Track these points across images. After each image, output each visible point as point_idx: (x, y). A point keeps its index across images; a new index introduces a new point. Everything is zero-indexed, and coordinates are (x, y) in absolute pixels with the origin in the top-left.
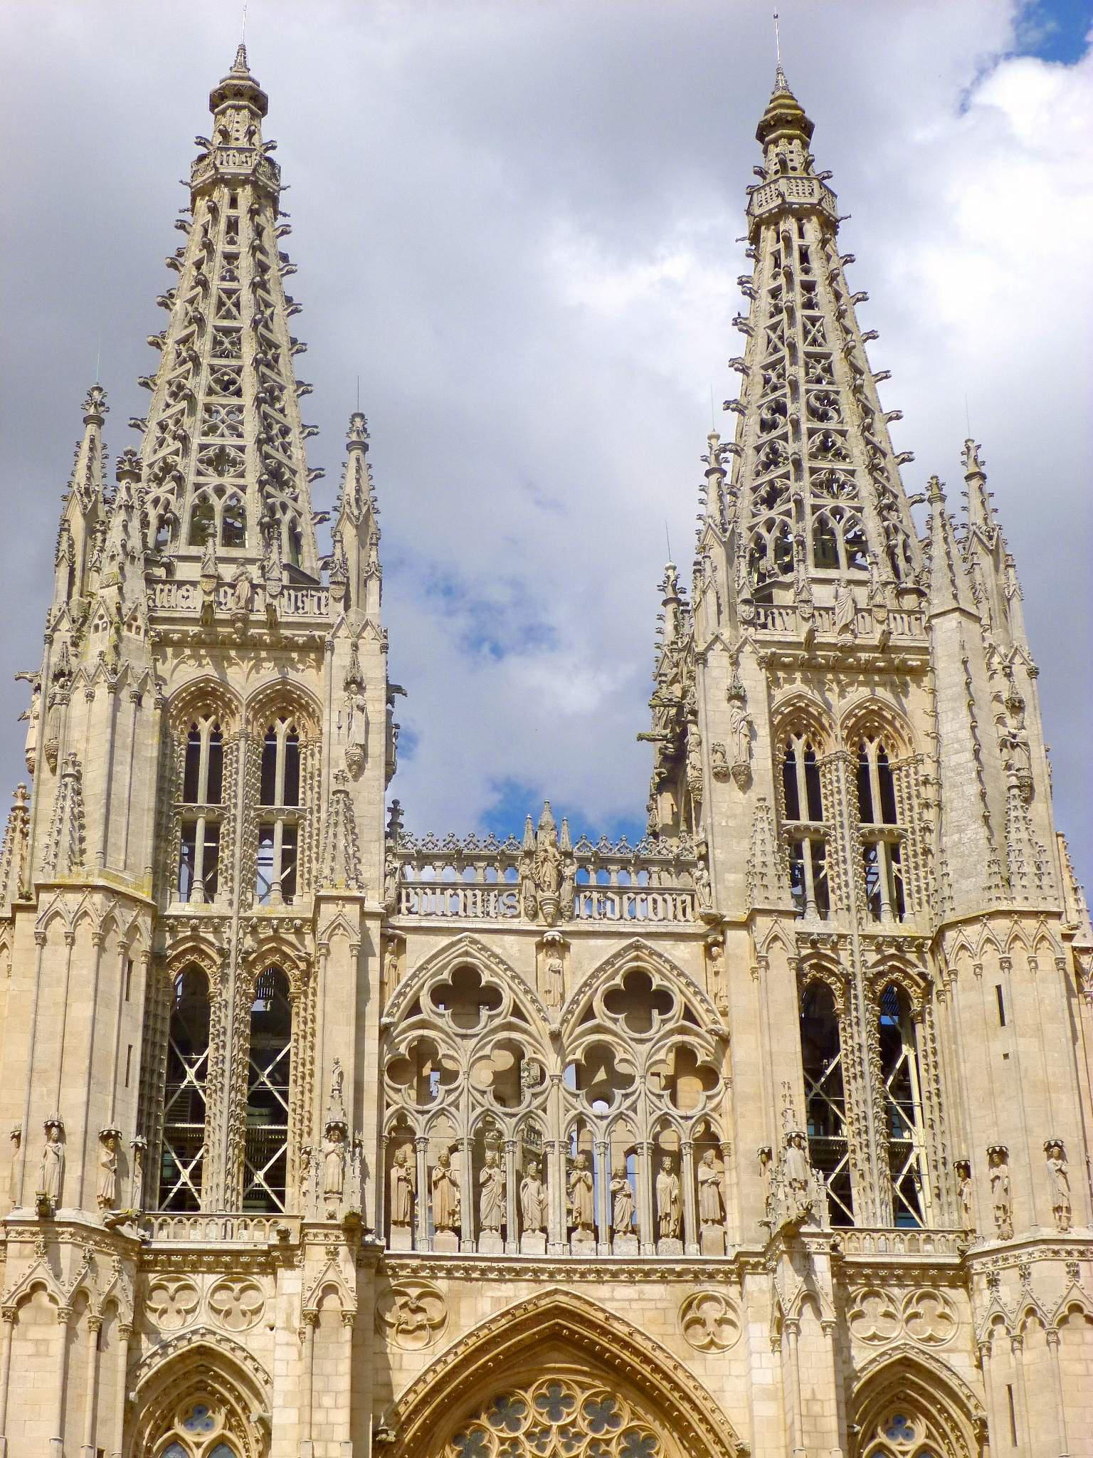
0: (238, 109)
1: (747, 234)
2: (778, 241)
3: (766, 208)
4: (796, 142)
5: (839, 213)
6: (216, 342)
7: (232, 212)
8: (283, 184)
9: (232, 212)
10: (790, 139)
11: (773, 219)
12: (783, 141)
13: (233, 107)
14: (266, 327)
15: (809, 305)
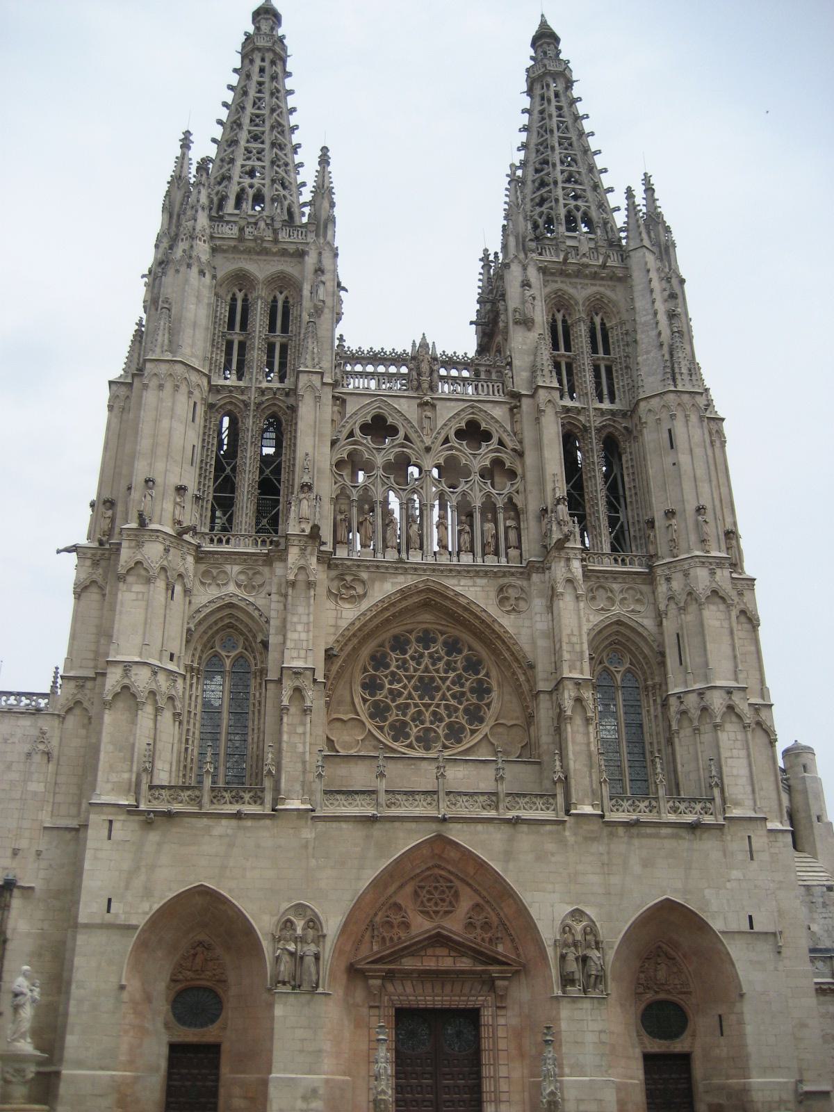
0: (267, 19)
1: (526, 90)
2: (543, 88)
3: (537, 73)
4: (552, 46)
5: (574, 79)
6: (251, 120)
7: (263, 64)
8: (288, 54)
9: (263, 64)
10: (549, 44)
11: (541, 78)
12: (545, 46)
13: (264, 19)
14: (278, 115)
15: (560, 116)
